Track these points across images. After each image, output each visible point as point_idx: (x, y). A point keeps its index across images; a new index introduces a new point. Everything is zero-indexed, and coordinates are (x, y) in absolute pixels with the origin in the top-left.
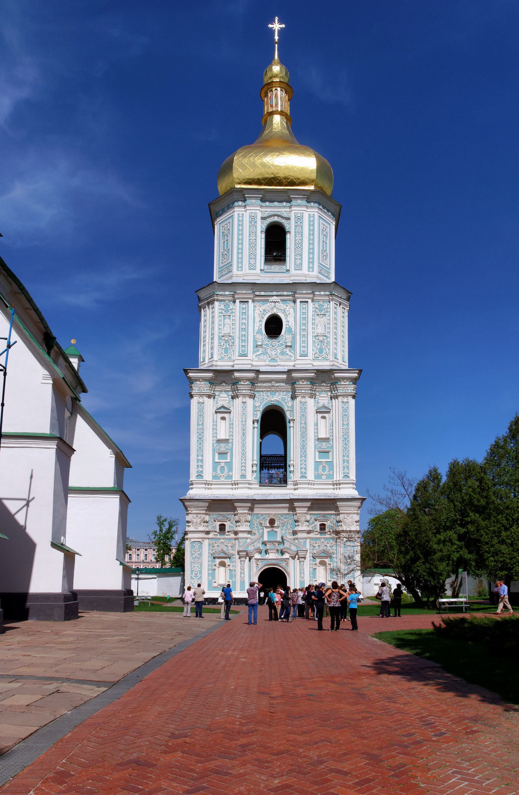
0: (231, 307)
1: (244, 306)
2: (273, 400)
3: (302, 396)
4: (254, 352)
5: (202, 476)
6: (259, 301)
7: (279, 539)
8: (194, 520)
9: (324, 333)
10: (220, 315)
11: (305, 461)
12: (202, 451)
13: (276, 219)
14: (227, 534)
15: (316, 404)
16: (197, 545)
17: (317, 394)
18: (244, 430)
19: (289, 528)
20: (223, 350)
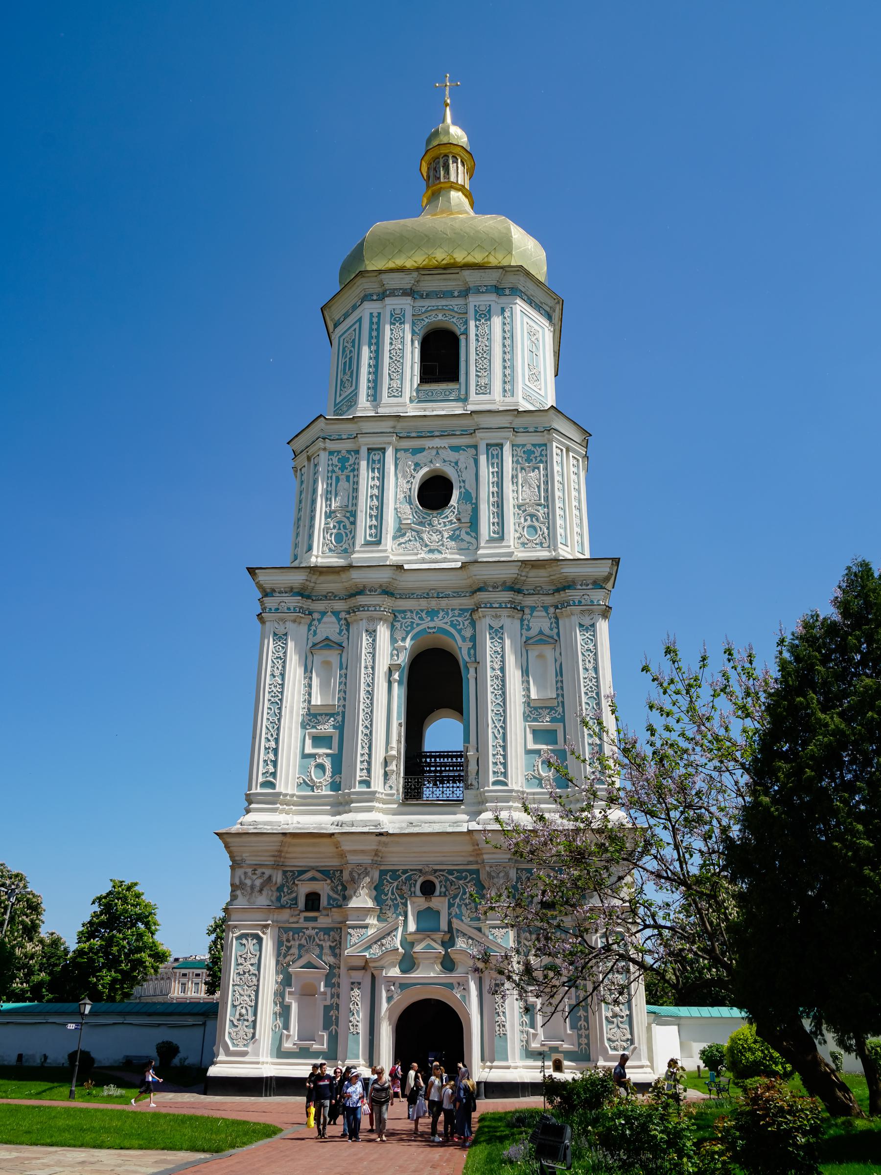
0: (351, 461)
1: (376, 458)
2: (431, 625)
3: (494, 614)
4: (395, 538)
5: (272, 785)
6: (406, 450)
7: (444, 926)
8: (248, 882)
9: (536, 498)
10: (330, 475)
11: (504, 748)
12: (278, 729)
13: (440, 317)
14: (324, 912)
15: (524, 632)
16: (251, 944)
17: (527, 611)
18: (369, 685)
19: (467, 901)
20: (333, 536)
